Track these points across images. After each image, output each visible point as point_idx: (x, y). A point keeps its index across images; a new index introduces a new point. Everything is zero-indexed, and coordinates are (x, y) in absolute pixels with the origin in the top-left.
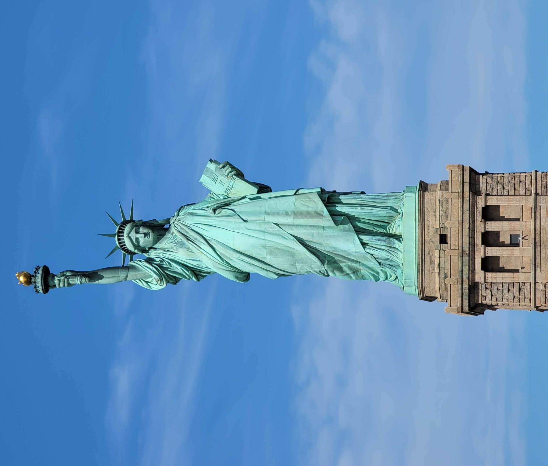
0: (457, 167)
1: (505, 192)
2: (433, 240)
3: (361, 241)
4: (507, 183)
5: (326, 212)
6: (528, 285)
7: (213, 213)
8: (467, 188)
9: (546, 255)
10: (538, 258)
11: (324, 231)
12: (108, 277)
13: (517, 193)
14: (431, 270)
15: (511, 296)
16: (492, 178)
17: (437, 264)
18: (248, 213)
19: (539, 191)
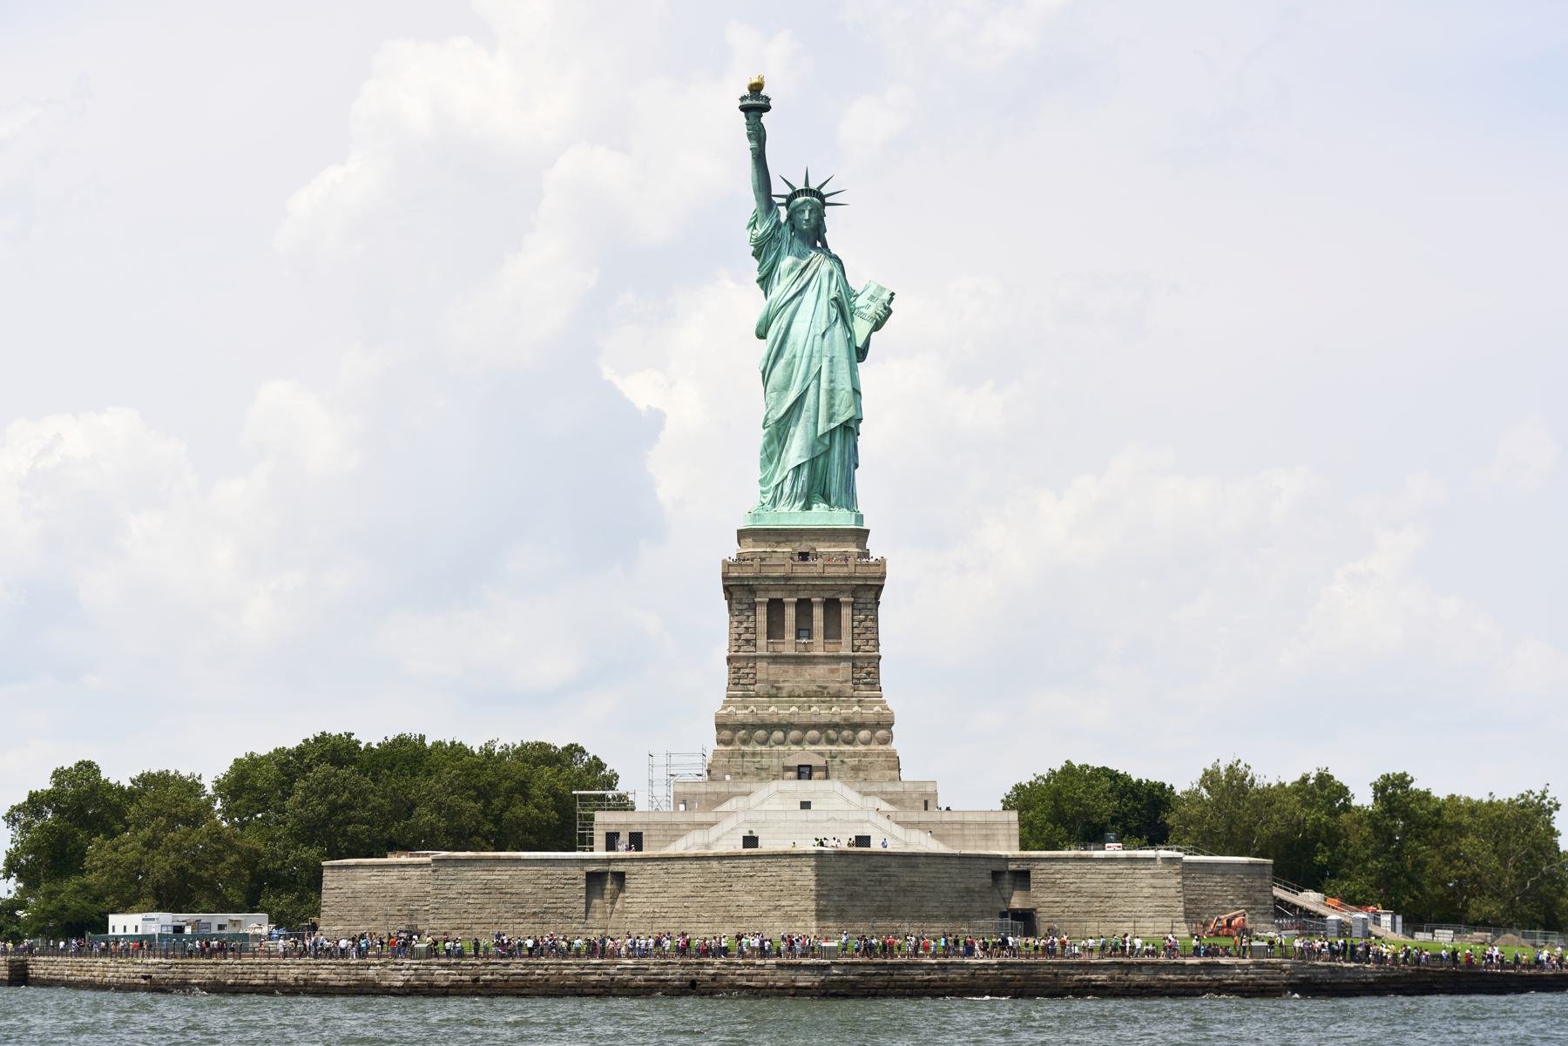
2: (803, 546)
5: (833, 425)
6: (753, 649)
10: (783, 660)
15: (741, 630)
17: (775, 550)
18: (832, 337)
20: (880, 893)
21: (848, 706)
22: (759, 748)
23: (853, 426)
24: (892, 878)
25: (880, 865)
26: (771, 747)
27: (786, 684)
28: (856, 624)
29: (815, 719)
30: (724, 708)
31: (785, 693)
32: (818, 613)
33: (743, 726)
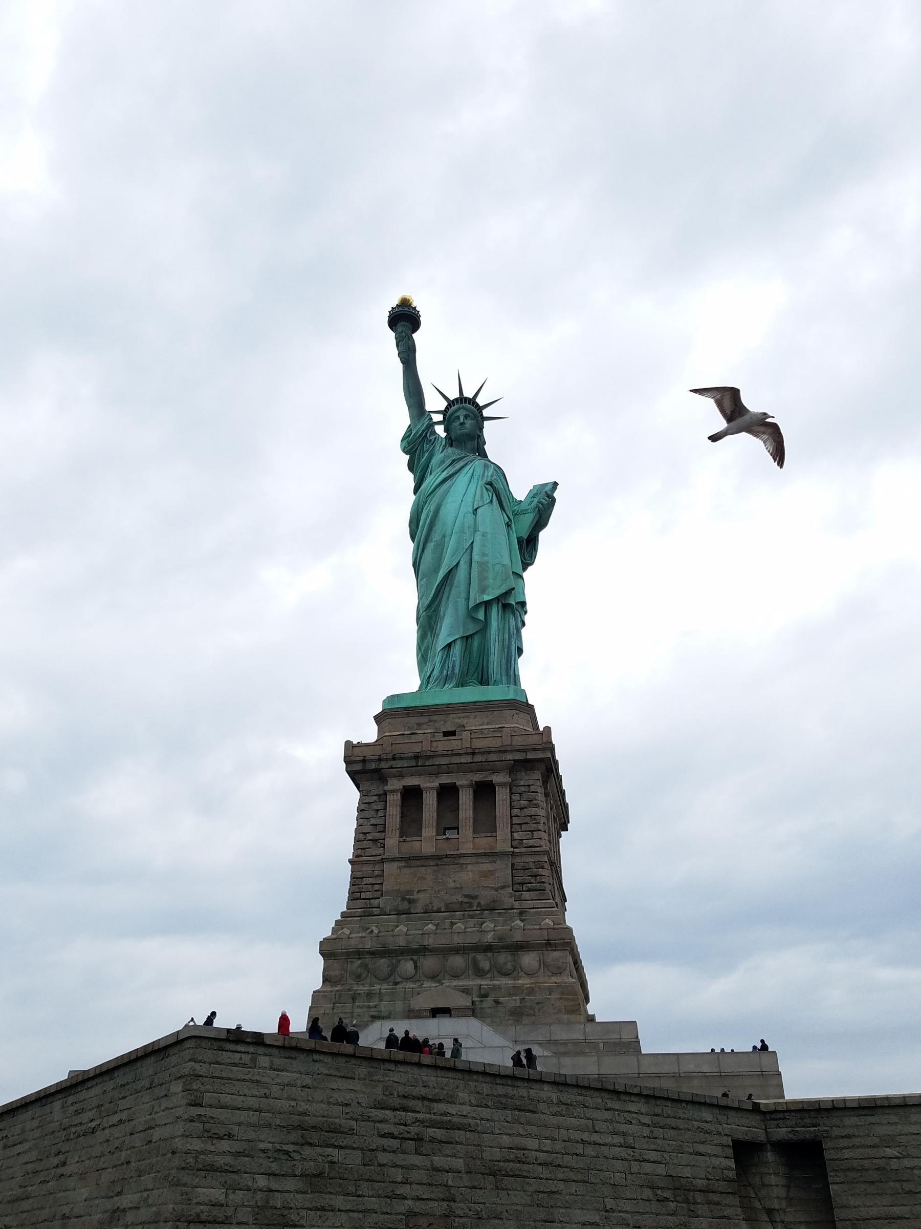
0: (546, 739)
1: (516, 810)
3: (453, 643)
4: (528, 813)
5: (486, 598)
6: (381, 851)
7: (487, 482)
8: (519, 756)
9: (424, 873)
10: (418, 863)
11: (463, 599)
12: (409, 386)
13: (516, 827)
14: (409, 725)
16: (536, 792)
17: (415, 732)
19: (518, 860)
20: (415, 1175)
21: (506, 920)
22: (377, 987)
23: (513, 603)
24: (459, 1135)
25: (424, 1092)
26: (396, 984)
27: (421, 896)
28: (515, 812)
29: (457, 940)
30: (334, 930)
31: (419, 907)
32: (466, 799)
33: (358, 954)
